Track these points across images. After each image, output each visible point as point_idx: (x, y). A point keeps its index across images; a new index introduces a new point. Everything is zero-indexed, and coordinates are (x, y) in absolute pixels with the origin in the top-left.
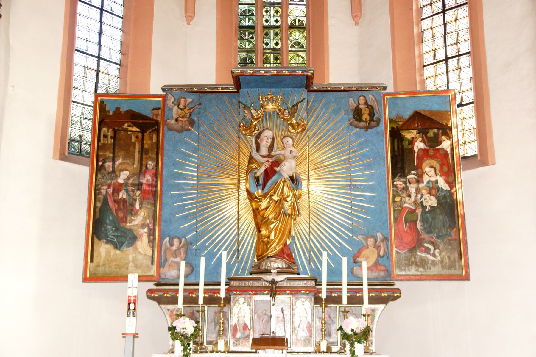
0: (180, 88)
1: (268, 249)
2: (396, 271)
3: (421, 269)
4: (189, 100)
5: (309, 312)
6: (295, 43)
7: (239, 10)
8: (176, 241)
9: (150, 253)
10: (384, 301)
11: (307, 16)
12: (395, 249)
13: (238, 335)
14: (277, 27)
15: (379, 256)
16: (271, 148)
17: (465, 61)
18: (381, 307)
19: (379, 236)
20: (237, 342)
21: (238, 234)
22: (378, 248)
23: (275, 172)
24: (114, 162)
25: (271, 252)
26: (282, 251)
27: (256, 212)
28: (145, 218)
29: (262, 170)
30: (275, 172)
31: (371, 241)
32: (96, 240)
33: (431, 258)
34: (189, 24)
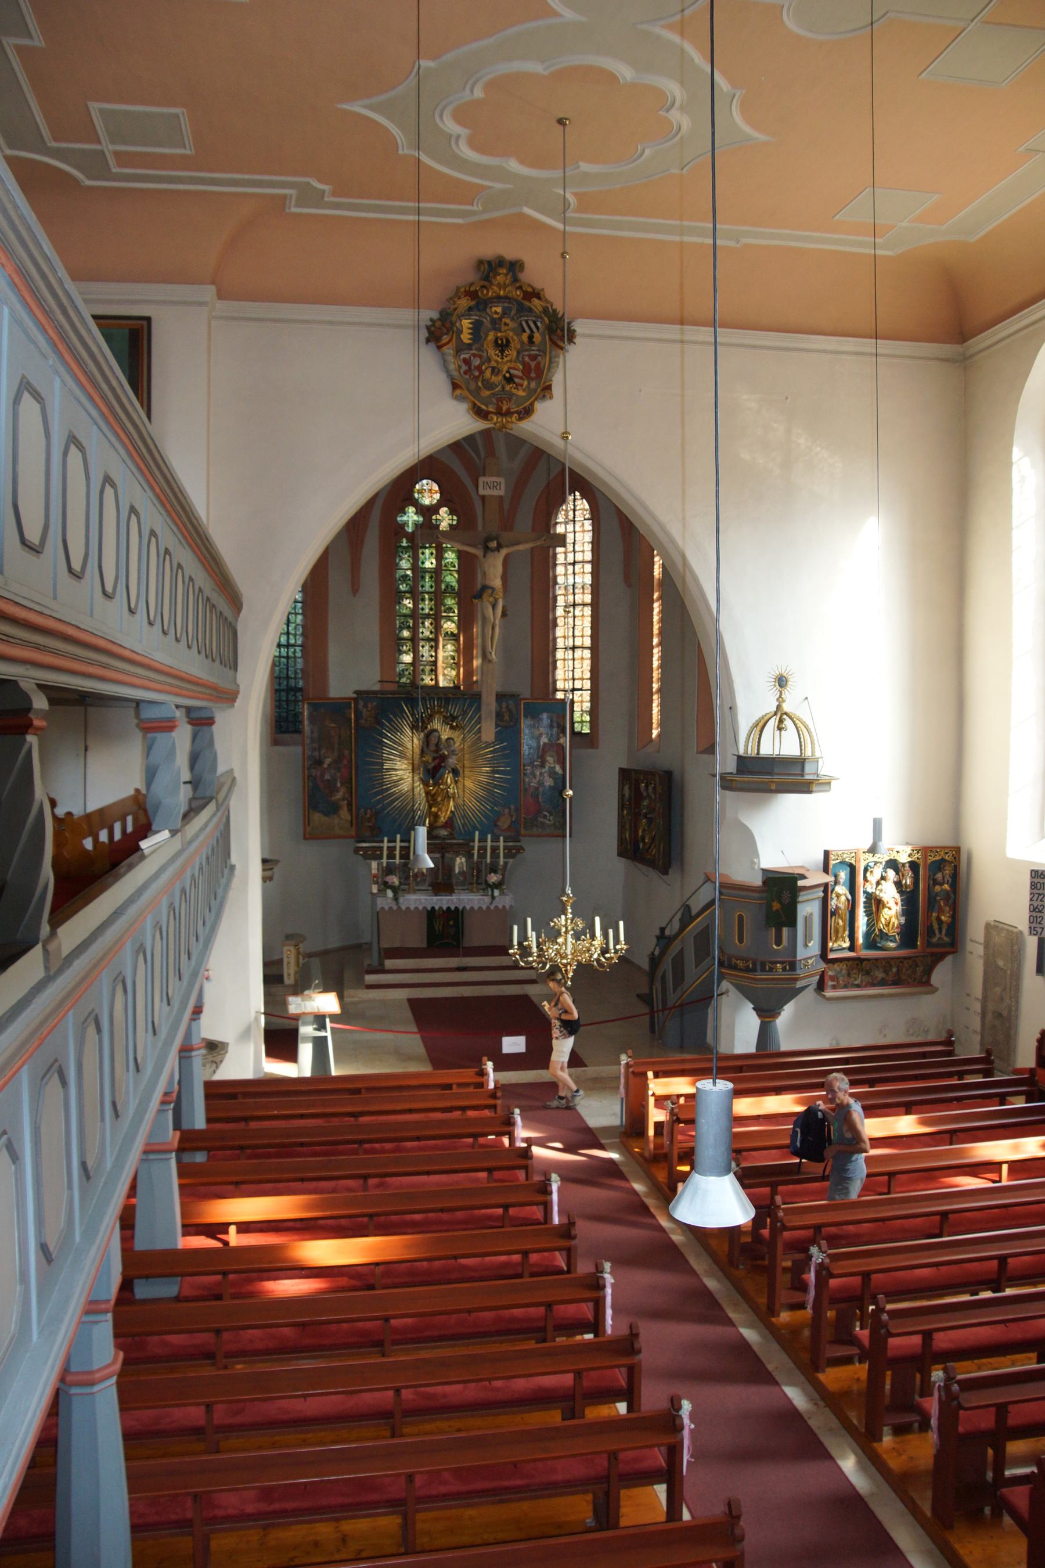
0: (367, 692)
1: (436, 821)
2: (523, 831)
3: (540, 830)
4: (375, 704)
5: (465, 864)
6: (448, 609)
7: (397, 576)
8: (369, 811)
9: (349, 818)
10: (513, 856)
11: (459, 581)
12: (523, 816)
13: (419, 879)
14: (431, 593)
15: (512, 821)
16: (437, 745)
17: (587, 654)
18: (511, 860)
19: (512, 807)
20: (418, 884)
21: (413, 806)
22: (511, 816)
23: (441, 767)
24: (319, 751)
25: (439, 824)
26: (446, 822)
27: (427, 793)
28: (344, 793)
29: (433, 765)
30: (441, 767)
31: (507, 811)
32: (311, 811)
33: (548, 822)
34: (354, 596)
